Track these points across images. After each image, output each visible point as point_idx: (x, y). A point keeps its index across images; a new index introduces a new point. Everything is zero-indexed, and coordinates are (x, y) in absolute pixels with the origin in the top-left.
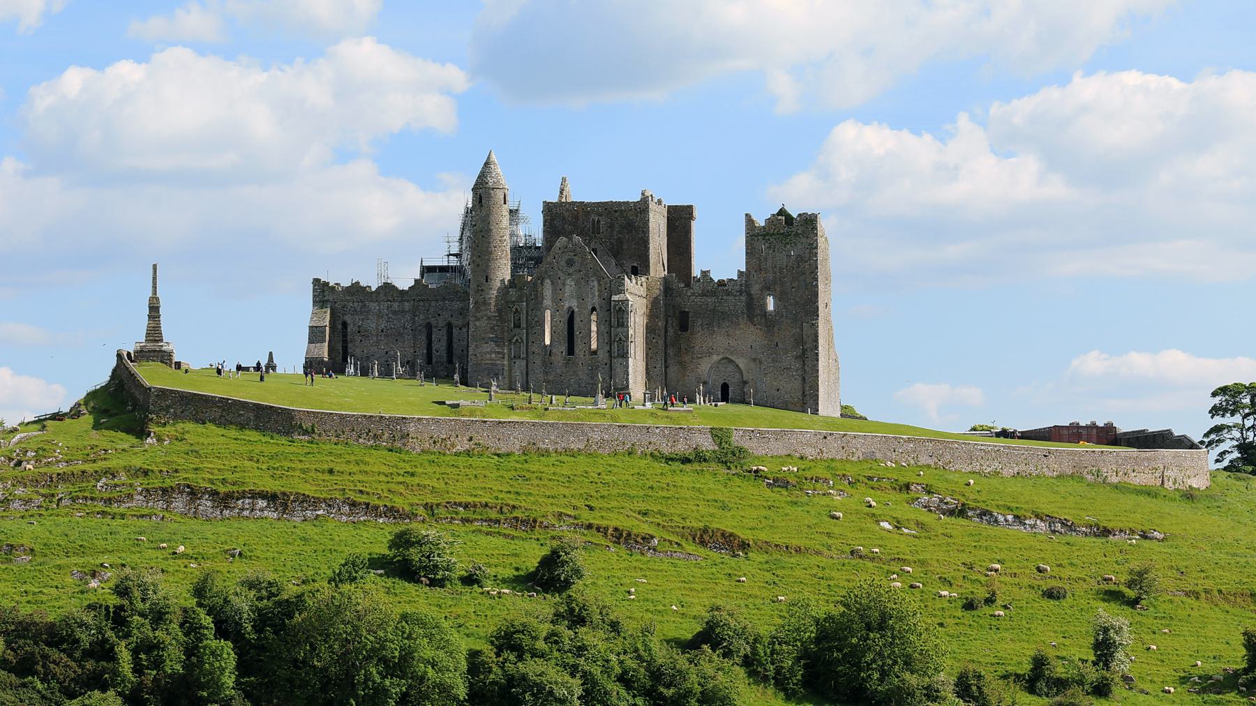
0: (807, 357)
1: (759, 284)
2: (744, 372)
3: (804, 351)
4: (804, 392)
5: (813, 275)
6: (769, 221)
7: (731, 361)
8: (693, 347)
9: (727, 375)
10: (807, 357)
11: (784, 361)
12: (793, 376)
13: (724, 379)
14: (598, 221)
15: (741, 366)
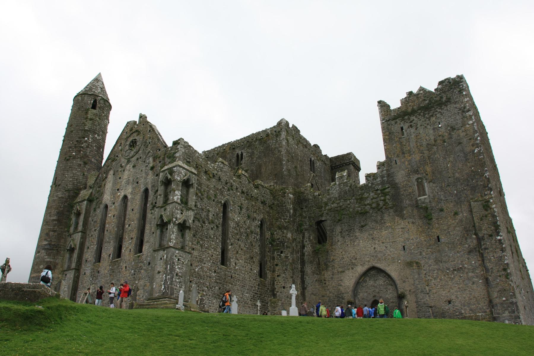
0: (486, 249)
1: (403, 170)
2: (398, 282)
3: (480, 240)
4: (490, 301)
5: (472, 141)
6: (405, 102)
7: (380, 271)
8: (333, 260)
9: (377, 290)
10: (486, 249)
11: (451, 259)
12: (468, 279)
13: (374, 296)
14: (242, 154)
15: (394, 275)
